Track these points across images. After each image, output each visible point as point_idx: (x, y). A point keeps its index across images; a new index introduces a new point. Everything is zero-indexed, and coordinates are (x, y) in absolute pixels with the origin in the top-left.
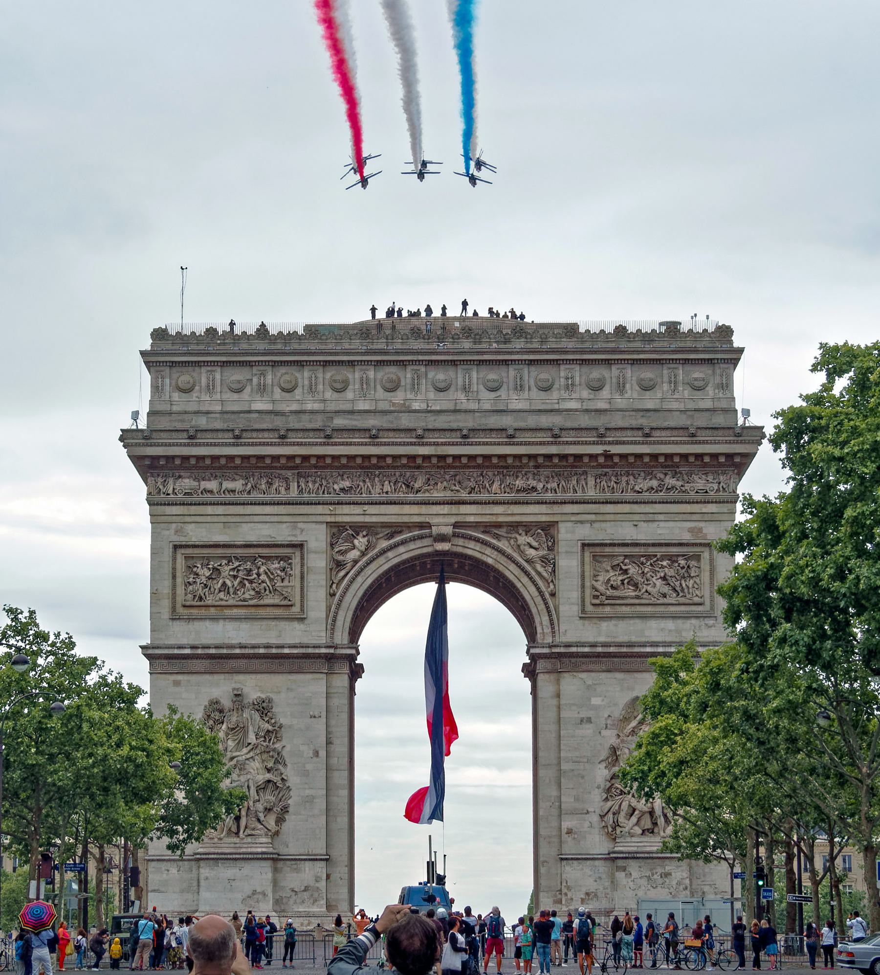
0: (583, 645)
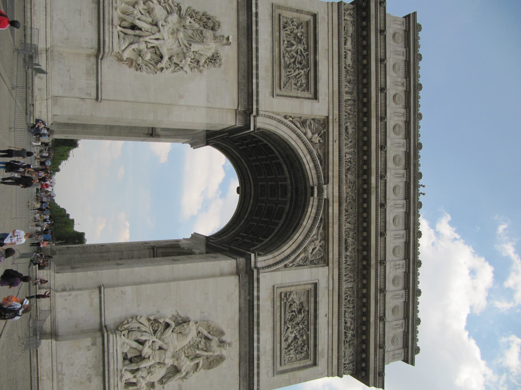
0: (258, 291)
